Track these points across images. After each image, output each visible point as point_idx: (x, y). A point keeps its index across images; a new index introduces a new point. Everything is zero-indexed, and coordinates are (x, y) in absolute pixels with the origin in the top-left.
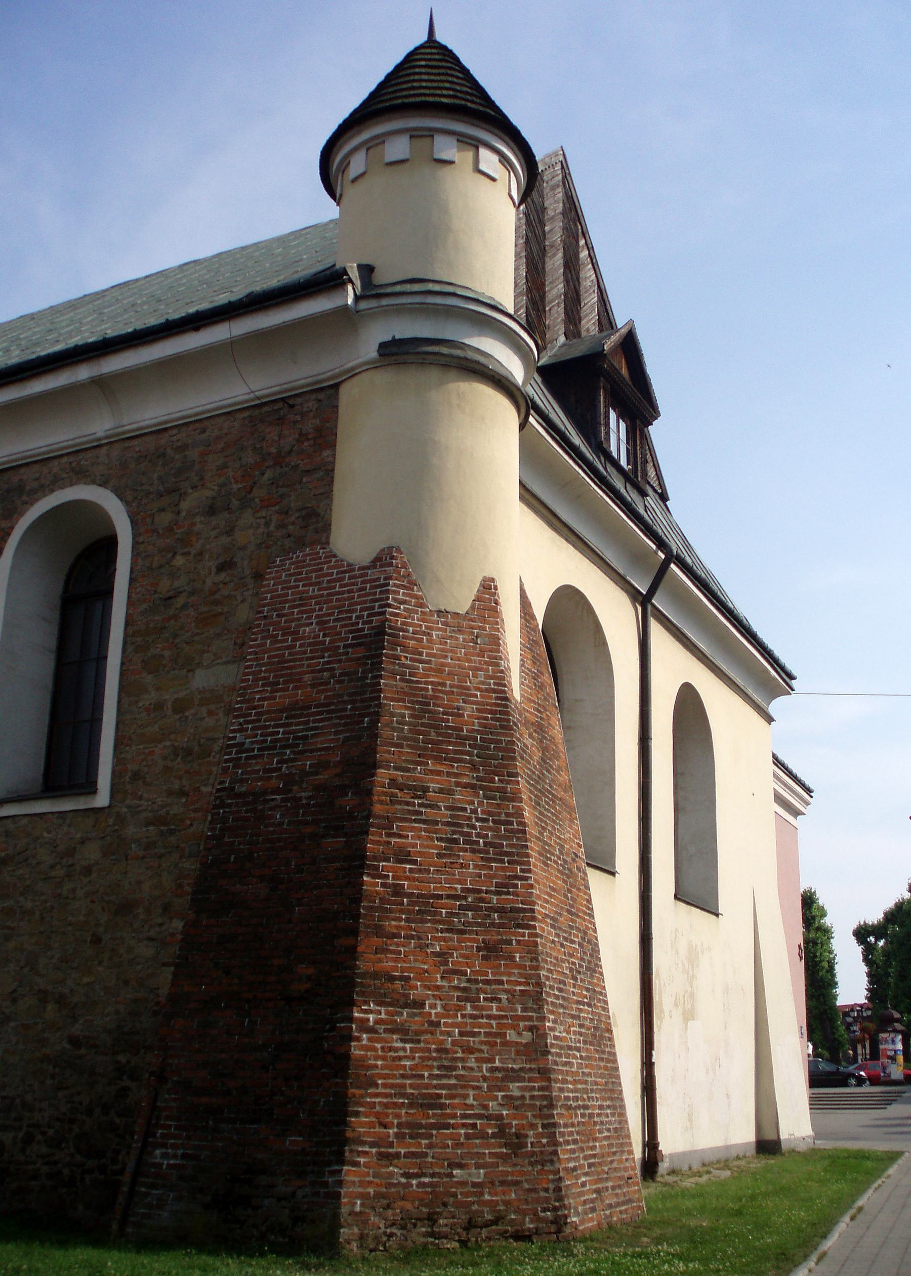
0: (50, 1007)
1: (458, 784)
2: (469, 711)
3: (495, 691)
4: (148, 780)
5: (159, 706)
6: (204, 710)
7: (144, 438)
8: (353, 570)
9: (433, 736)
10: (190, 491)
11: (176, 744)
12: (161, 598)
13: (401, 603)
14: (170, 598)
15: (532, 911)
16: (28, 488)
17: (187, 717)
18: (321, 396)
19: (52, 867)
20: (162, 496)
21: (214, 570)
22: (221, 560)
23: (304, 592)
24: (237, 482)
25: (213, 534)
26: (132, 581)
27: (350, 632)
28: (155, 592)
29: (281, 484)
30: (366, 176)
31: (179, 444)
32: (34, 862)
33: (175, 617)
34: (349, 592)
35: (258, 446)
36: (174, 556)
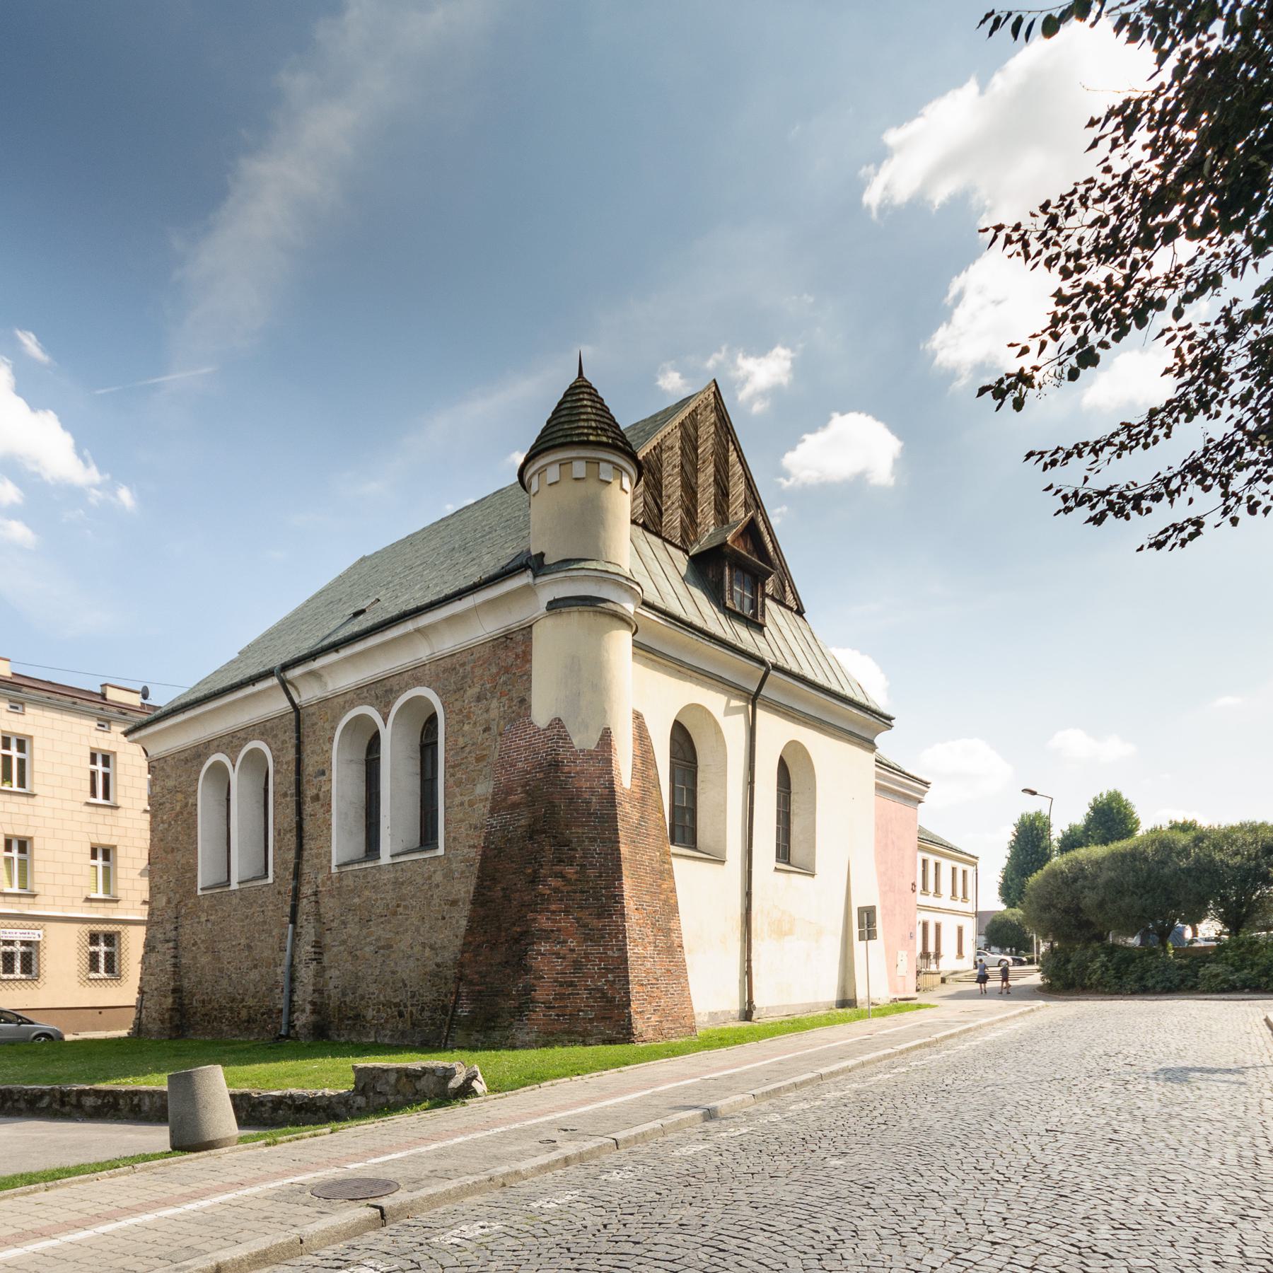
5: (462, 804)
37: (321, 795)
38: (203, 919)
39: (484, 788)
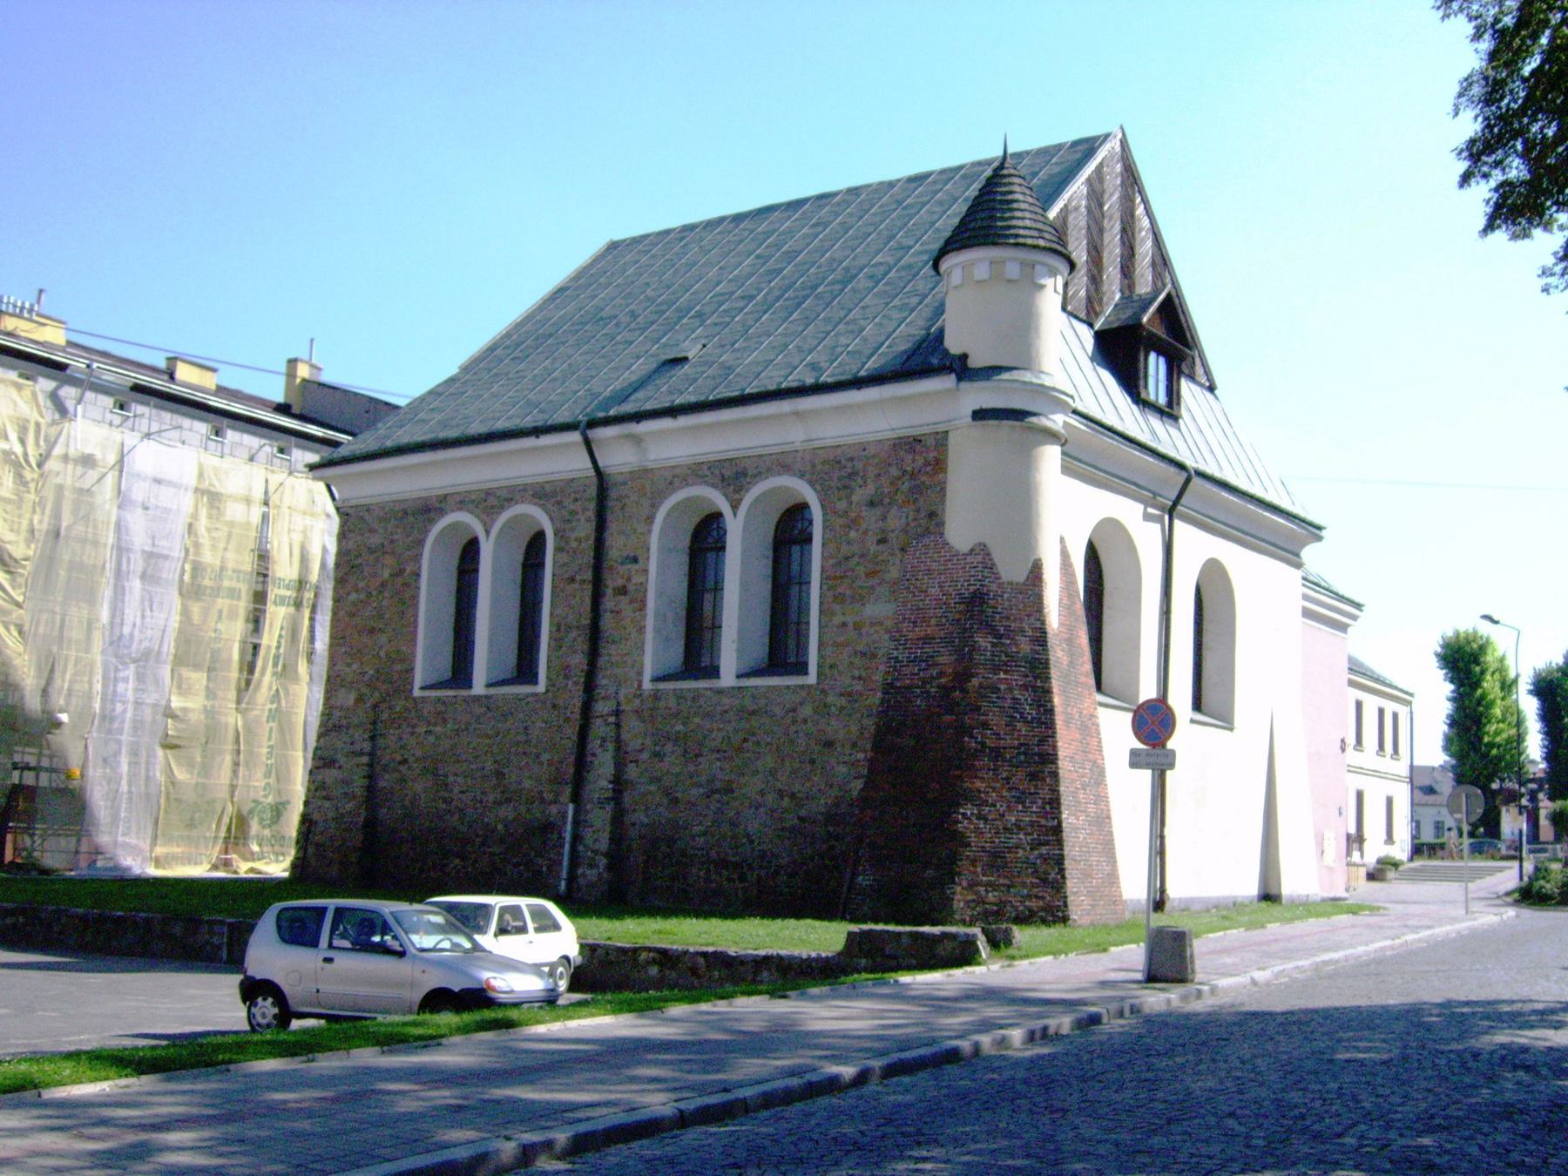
0: (786, 799)
5: (844, 625)
37: (631, 587)
38: (421, 729)
39: (880, 609)
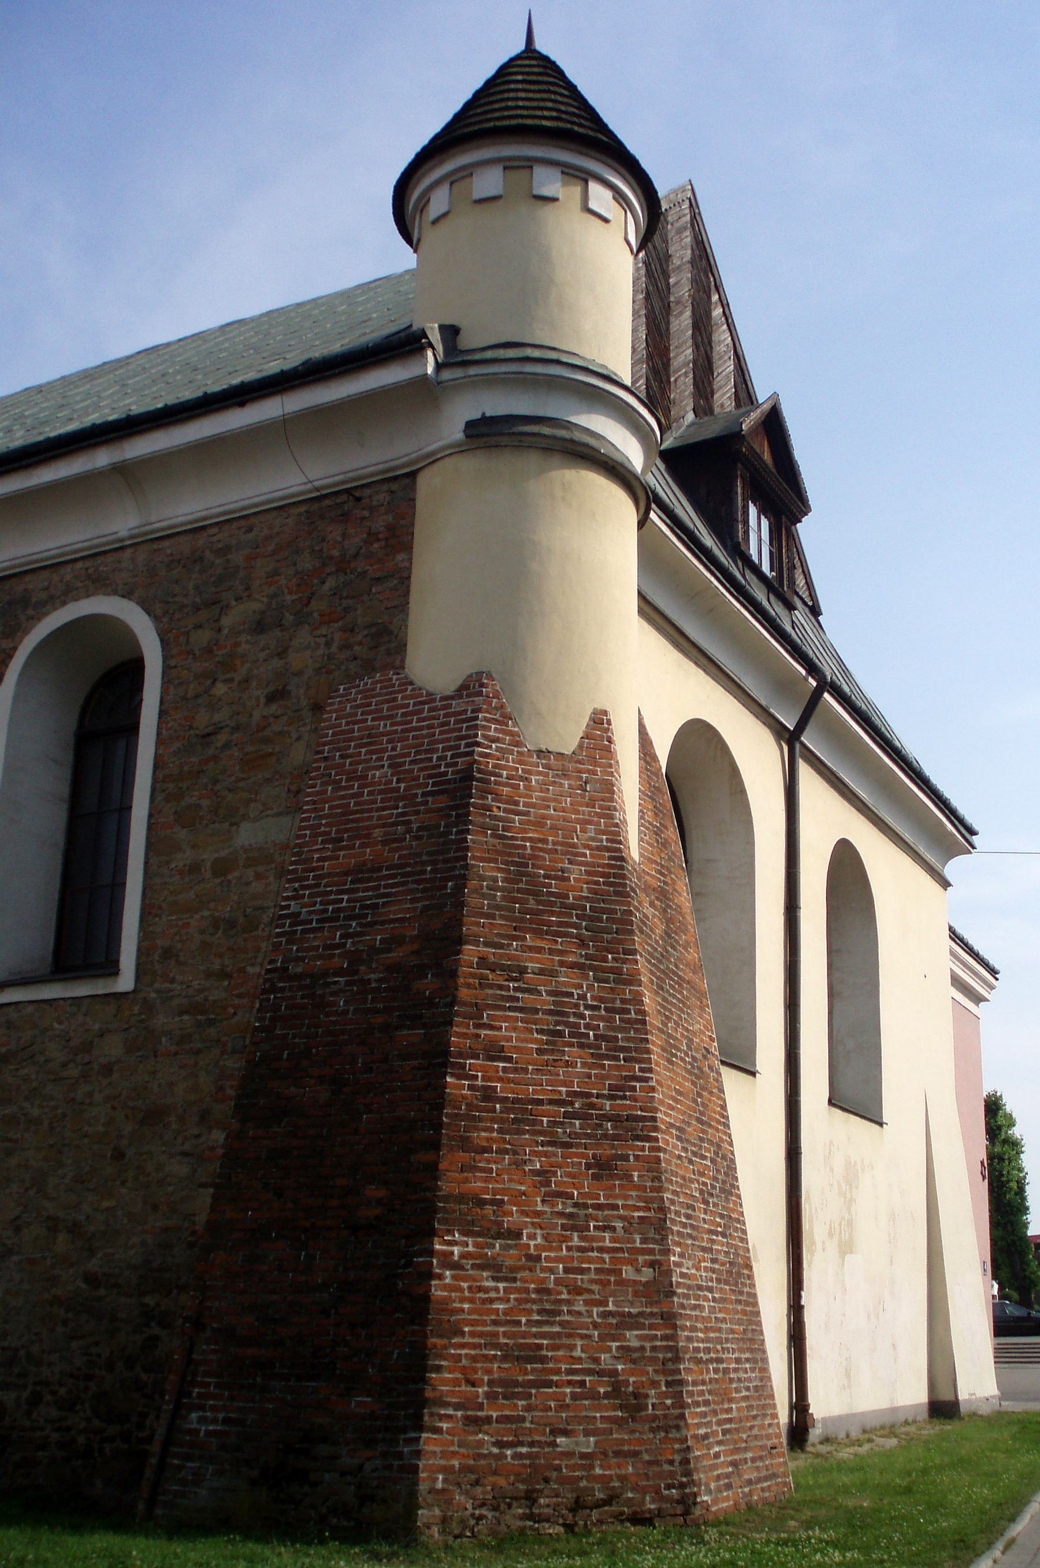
0: (62, 1237)
1: (562, 964)
2: (575, 873)
3: (608, 849)
4: (182, 958)
5: (195, 868)
6: (250, 873)
7: (177, 538)
8: (434, 700)
9: (532, 904)
10: (234, 603)
11: (216, 914)
12: (197, 736)
13: (493, 741)
14: (209, 735)
15: (654, 1119)
16: (34, 600)
17: (229, 881)
18: (394, 486)
19: (64, 1065)
20: (198, 609)
21: (263, 700)
22: (271, 688)
23: (373, 727)
24: (290, 592)
25: (262, 656)
26: (162, 713)
27: (430, 776)
28: (191, 727)
29: (345, 594)
30: (450, 216)
31: (220, 545)
32: (42, 1059)
33: (215, 758)
34: (429, 727)
35: (317, 548)
36: (214, 683)
